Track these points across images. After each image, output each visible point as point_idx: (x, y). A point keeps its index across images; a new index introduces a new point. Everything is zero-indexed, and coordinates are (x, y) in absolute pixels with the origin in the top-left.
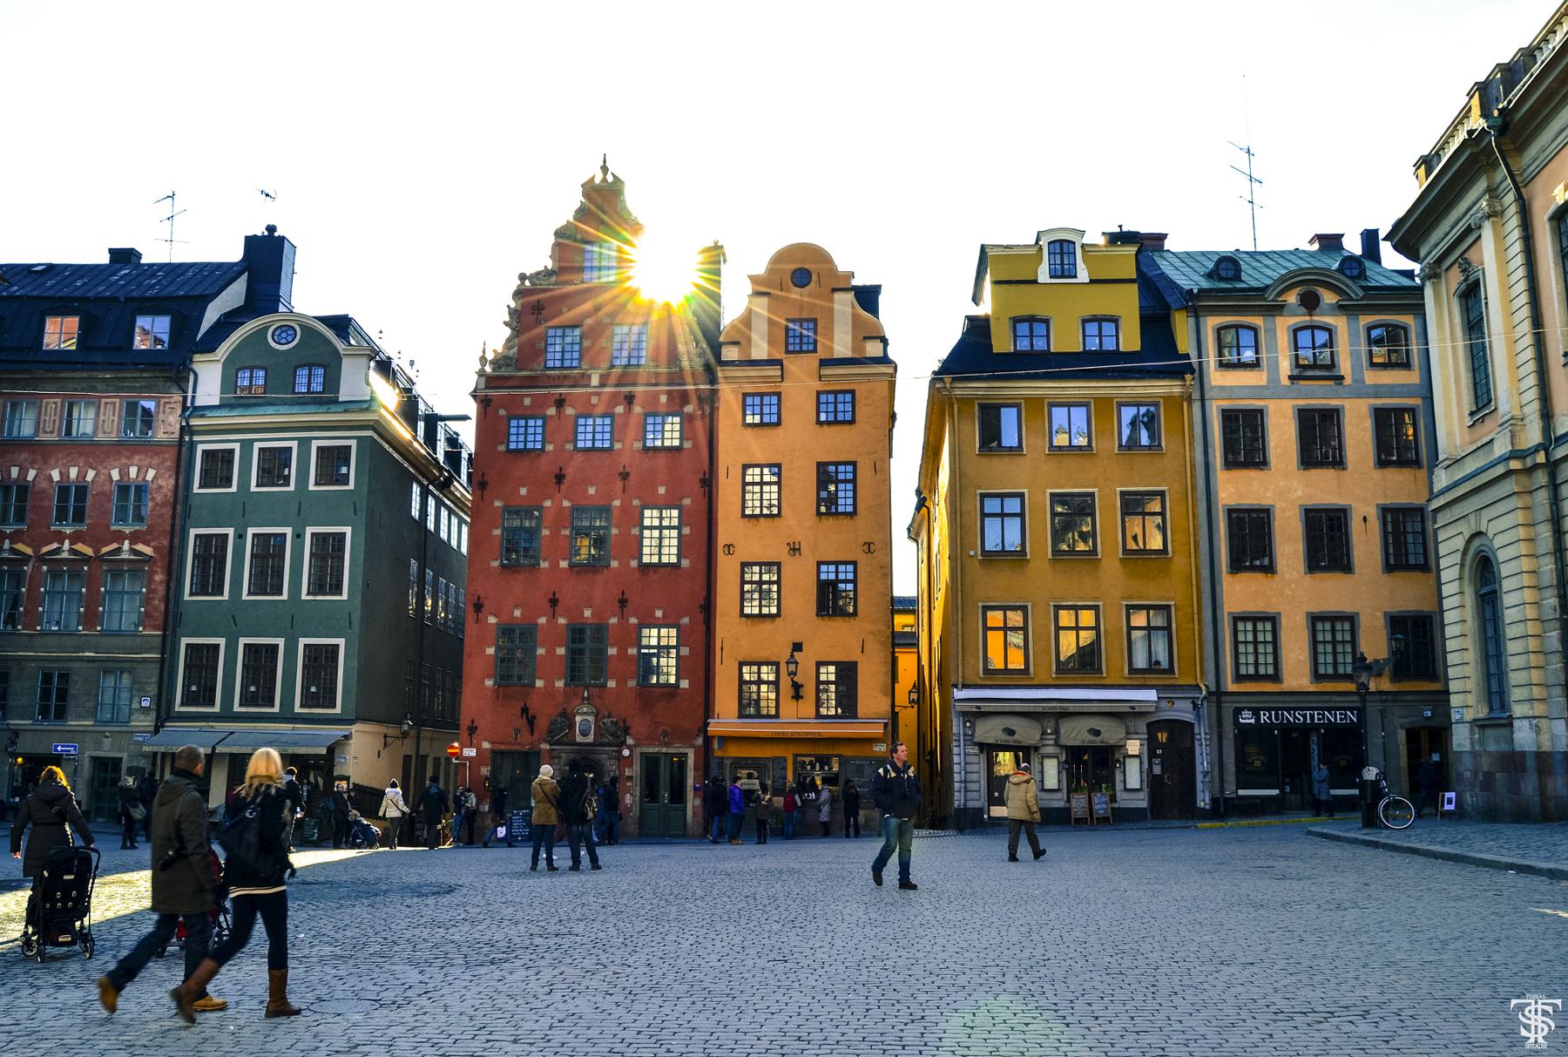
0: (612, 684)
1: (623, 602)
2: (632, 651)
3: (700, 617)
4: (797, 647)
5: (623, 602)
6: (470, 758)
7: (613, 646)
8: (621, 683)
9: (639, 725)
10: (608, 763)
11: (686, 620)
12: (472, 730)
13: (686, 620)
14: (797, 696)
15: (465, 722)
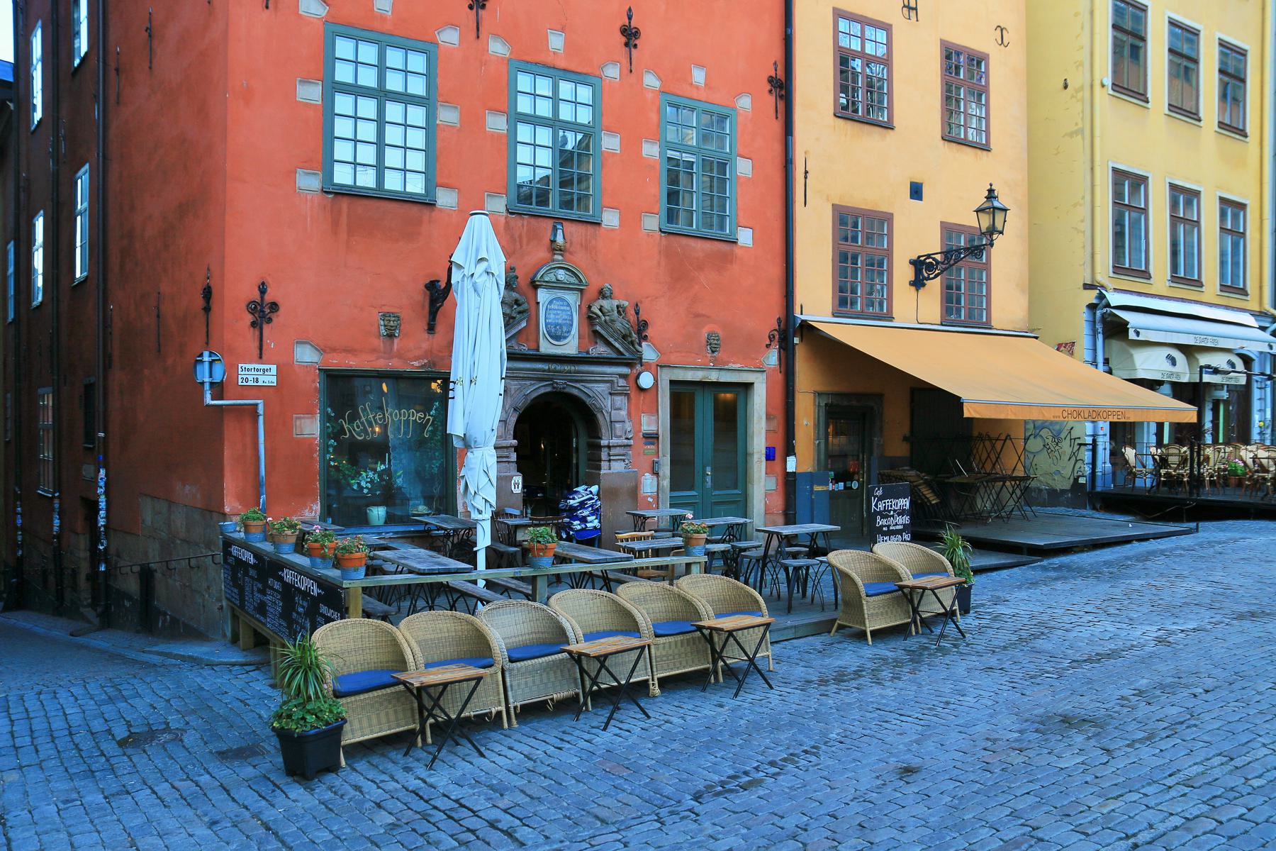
0: (610, 219)
1: (630, 35)
2: (651, 150)
3: (770, 101)
4: (916, 191)
5: (630, 35)
6: (259, 390)
7: (611, 130)
8: (630, 219)
9: (665, 321)
10: (607, 403)
11: (745, 102)
12: (263, 312)
13: (745, 102)
14: (918, 283)
15: (236, 292)
